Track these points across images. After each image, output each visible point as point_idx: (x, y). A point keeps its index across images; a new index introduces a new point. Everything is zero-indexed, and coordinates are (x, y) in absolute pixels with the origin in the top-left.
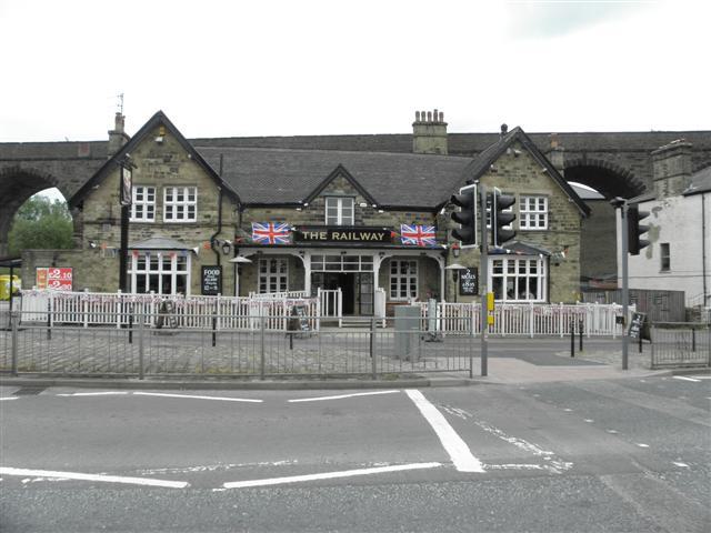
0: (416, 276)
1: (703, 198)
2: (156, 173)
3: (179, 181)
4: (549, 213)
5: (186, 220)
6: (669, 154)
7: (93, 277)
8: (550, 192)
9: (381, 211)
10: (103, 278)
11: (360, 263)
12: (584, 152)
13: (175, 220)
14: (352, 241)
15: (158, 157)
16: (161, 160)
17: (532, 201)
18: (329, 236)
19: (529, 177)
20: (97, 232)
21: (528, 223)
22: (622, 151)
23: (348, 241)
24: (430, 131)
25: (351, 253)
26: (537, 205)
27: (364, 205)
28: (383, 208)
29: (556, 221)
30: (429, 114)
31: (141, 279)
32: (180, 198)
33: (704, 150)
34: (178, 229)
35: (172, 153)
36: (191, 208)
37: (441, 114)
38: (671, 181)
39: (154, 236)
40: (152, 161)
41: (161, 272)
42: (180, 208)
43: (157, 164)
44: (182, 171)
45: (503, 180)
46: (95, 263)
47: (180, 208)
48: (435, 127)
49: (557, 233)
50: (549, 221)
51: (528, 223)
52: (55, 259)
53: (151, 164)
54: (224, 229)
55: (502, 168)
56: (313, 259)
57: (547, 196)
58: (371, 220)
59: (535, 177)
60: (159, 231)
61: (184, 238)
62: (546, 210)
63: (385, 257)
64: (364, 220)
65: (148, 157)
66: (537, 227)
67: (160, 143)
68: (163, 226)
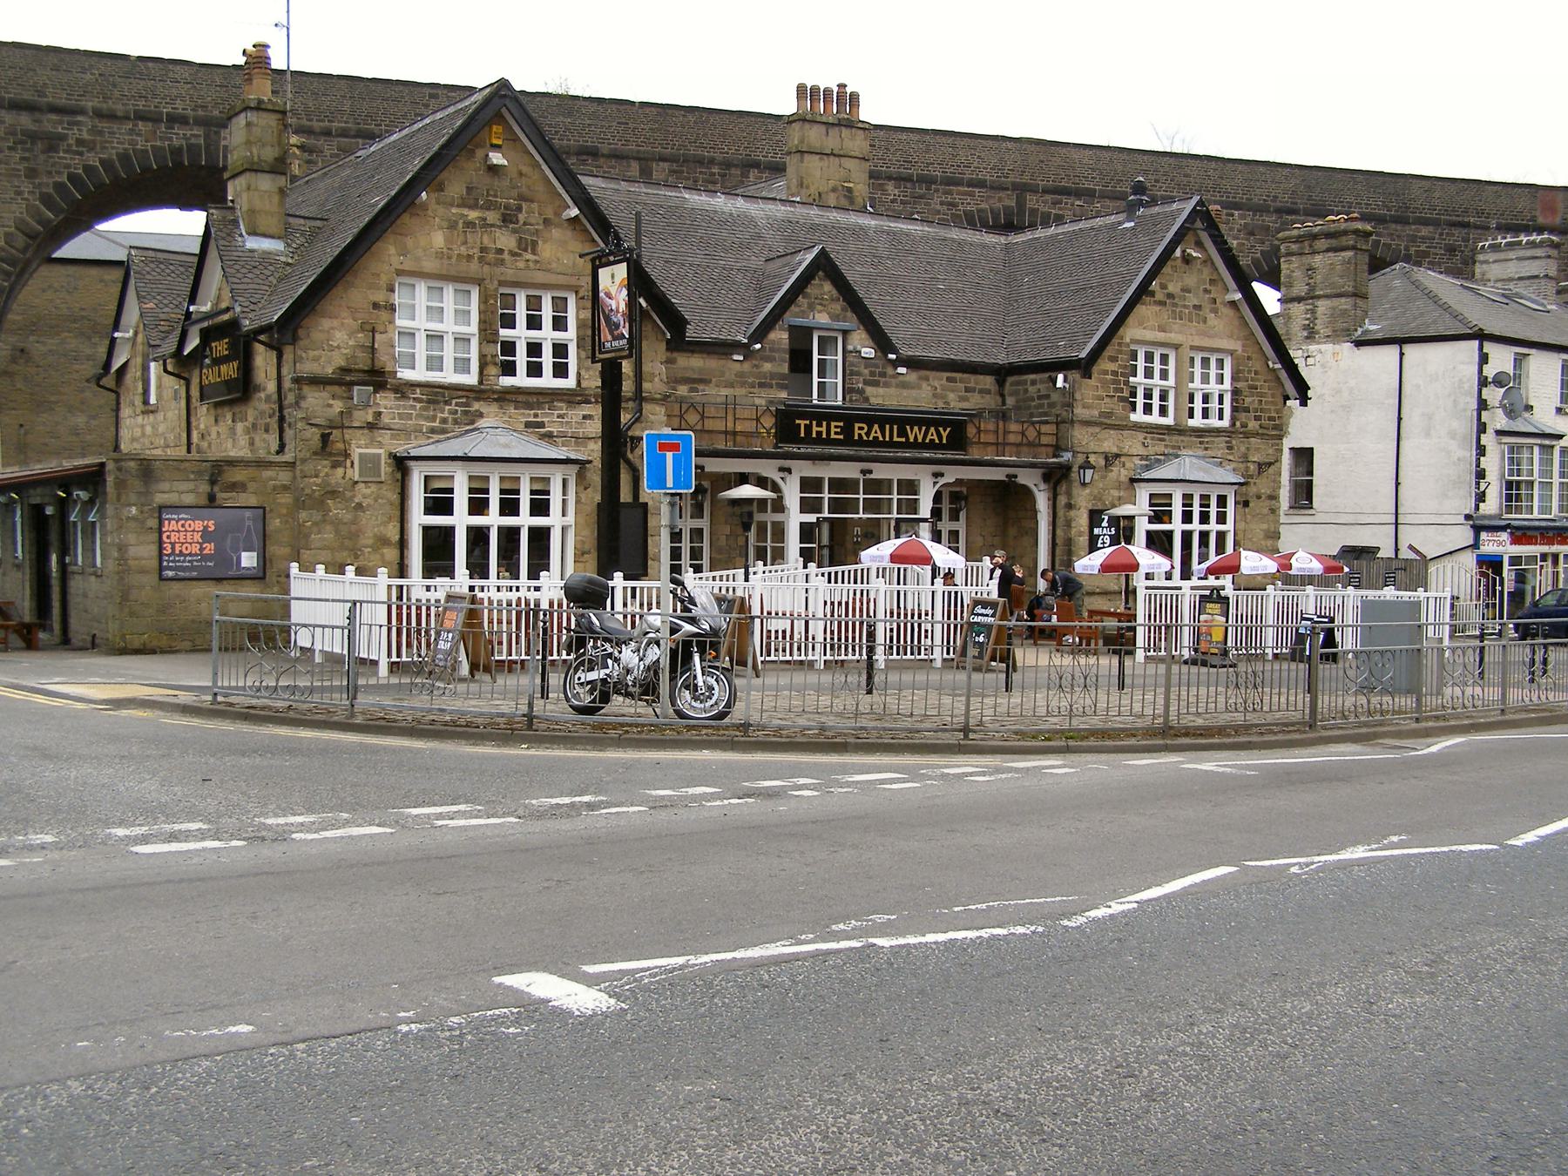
0: (704, 523)
1: (1402, 354)
2: (483, 249)
3: (540, 277)
4: (1236, 392)
5: (547, 381)
6: (1322, 244)
7: (328, 535)
8: (1237, 346)
9: (902, 370)
10: (355, 536)
11: (826, 495)
12: (1021, 189)
13: (521, 380)
14: (892, 444)
15: (489, 206)
16: (492, 217)
17: (1206, 362)
18: (847, 430)
19: (1206, 312)
20: (338, 406)
21: (1198, 412)
22: (1103, 196)
23: (884, 444)
24: (832, 141)
25: (881, 472)
26: (1213, 372)
27: (868, 352)
28: (913, 364)
29: (1247, 410)
30: (828, 92)
31: (478, 537)
32: (534, 323)
33: (1279, 211)
34: (539, 406)
35: (522, 198)
36: (560, 350)
37: (854, 98)
38: (1323, 306)
39: (481, 423)
40: (473, 215)
41: (525, 520)
42: (534, 349)
43: (485, 225)
44: (547, 251)
45: (1165, 314)
46: (333, 494)
47: (534, 349)
48: (845, 132)
49: (1247, 435)
50: (1234, 409)
51: (1198, 412)
52: (213, 482)
53: (470, 224)
54: (647, 407)
55: (1163, 287)
56: (808, 484)
57: (1232, 353)
58: (881, 391)
59: (1215, 311)
60: (493, 408)
61: (554, 430)
62: (1227, 385)
63: (942, 481)
64: (869, 390)
65: (462, 205)
66: (1214, 422)
67: (494, 169)
68: (508, 397)
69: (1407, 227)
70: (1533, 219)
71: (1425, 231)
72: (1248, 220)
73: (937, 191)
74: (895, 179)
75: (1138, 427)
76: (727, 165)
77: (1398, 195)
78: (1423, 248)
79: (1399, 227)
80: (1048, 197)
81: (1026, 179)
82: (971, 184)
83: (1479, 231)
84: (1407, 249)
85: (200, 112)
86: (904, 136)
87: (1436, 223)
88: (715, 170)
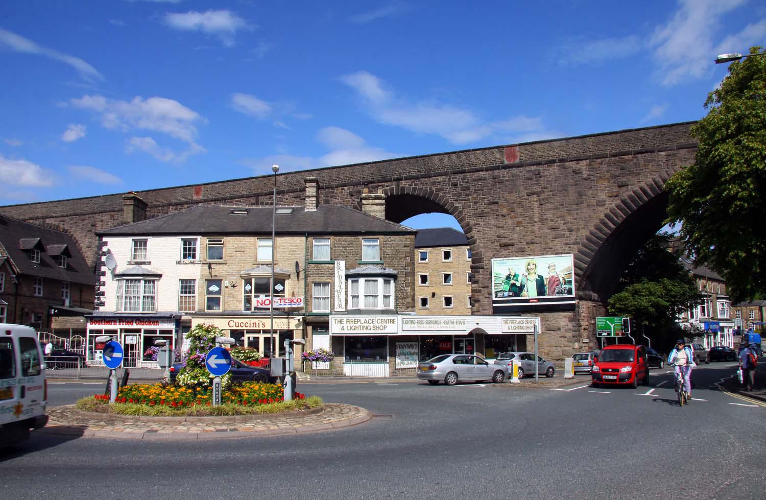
22: (288, 192)
69: (431, 179)
70: (502, 162)
71: (440, 179)
72: (351, 190)
73: (228, 202)
74: (213, 201)
75: (36, 297)
76: (164, 206)
77: (425, 165)
78: (439, 186)
79: (426, 179)
80: (268, 196)
81: (259, 191)
82: (239, 197)
83: (471, 174)
84: (431, 189)
85: (42, 215)
86: (217, 185)
87: (446, 174)
88: (160, 208)
